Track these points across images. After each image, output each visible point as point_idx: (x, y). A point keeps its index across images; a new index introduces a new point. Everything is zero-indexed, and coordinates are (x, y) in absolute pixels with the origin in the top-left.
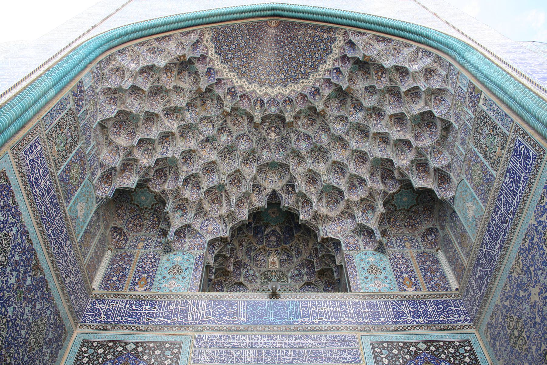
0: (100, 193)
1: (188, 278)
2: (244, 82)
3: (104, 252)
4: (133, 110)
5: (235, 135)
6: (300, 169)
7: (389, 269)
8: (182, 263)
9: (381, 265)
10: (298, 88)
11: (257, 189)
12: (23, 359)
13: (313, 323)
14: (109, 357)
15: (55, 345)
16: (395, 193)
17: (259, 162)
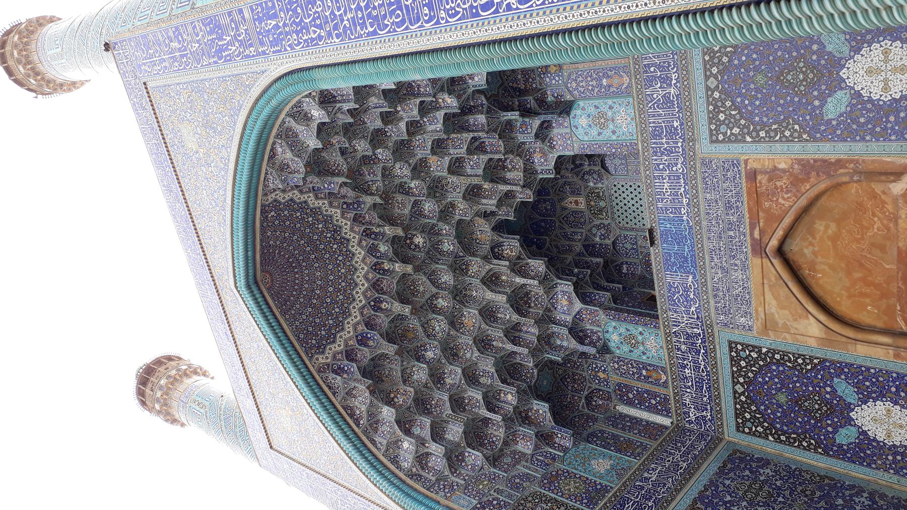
0: (568, 444)
1: (640, 329)
2: (357, 293)
3: (623, 416)
4: (461, 430)
5: (434, 290)
6: (462, 205)
7: (596, 102)
8: (620, 335)
9: (592, 110)
10: (346, 224)
11: (496, 250)
12: (783, 503)
13: (688, 204)
14: (753, 408)
15: (754, 465)
16: (485, 96)
17: (461, 254)
